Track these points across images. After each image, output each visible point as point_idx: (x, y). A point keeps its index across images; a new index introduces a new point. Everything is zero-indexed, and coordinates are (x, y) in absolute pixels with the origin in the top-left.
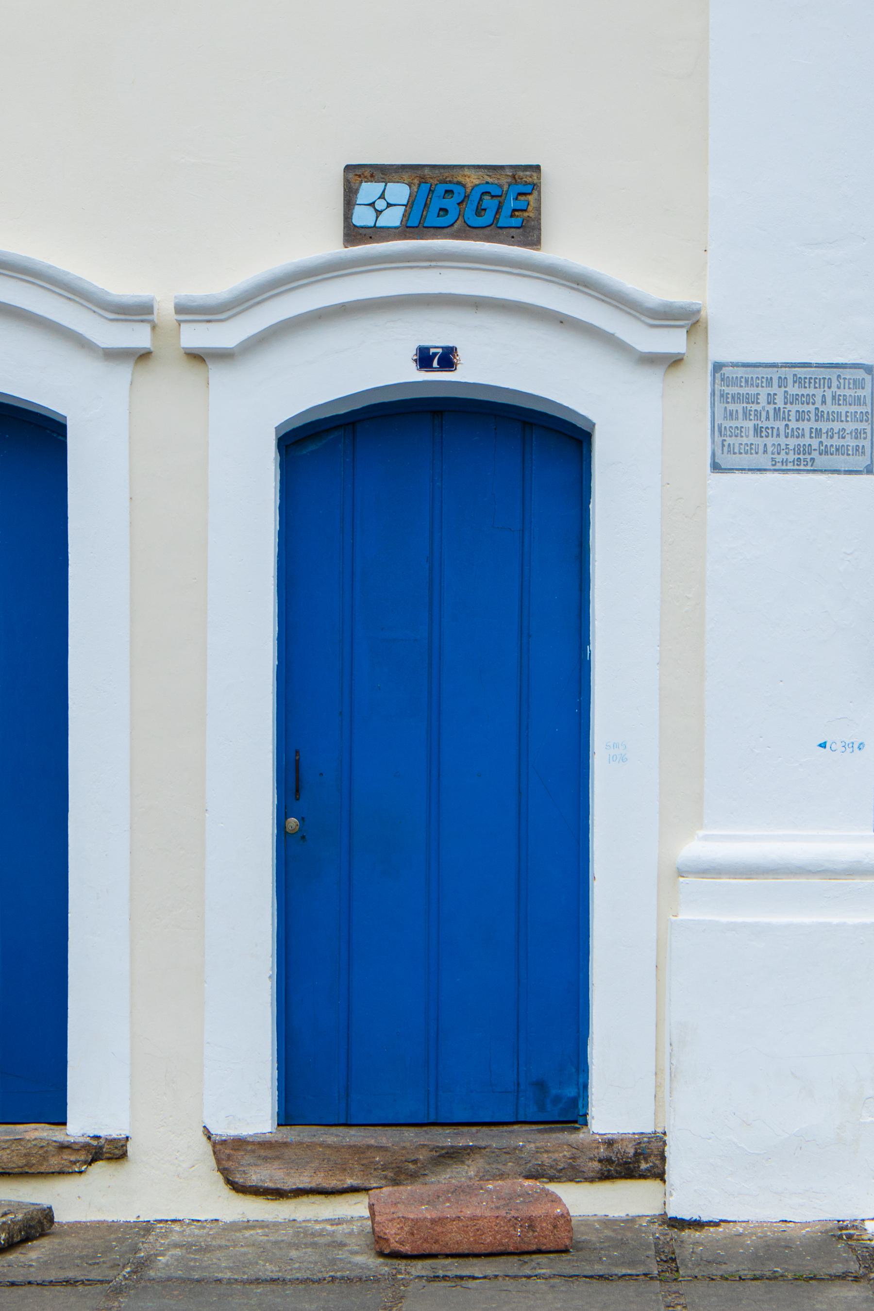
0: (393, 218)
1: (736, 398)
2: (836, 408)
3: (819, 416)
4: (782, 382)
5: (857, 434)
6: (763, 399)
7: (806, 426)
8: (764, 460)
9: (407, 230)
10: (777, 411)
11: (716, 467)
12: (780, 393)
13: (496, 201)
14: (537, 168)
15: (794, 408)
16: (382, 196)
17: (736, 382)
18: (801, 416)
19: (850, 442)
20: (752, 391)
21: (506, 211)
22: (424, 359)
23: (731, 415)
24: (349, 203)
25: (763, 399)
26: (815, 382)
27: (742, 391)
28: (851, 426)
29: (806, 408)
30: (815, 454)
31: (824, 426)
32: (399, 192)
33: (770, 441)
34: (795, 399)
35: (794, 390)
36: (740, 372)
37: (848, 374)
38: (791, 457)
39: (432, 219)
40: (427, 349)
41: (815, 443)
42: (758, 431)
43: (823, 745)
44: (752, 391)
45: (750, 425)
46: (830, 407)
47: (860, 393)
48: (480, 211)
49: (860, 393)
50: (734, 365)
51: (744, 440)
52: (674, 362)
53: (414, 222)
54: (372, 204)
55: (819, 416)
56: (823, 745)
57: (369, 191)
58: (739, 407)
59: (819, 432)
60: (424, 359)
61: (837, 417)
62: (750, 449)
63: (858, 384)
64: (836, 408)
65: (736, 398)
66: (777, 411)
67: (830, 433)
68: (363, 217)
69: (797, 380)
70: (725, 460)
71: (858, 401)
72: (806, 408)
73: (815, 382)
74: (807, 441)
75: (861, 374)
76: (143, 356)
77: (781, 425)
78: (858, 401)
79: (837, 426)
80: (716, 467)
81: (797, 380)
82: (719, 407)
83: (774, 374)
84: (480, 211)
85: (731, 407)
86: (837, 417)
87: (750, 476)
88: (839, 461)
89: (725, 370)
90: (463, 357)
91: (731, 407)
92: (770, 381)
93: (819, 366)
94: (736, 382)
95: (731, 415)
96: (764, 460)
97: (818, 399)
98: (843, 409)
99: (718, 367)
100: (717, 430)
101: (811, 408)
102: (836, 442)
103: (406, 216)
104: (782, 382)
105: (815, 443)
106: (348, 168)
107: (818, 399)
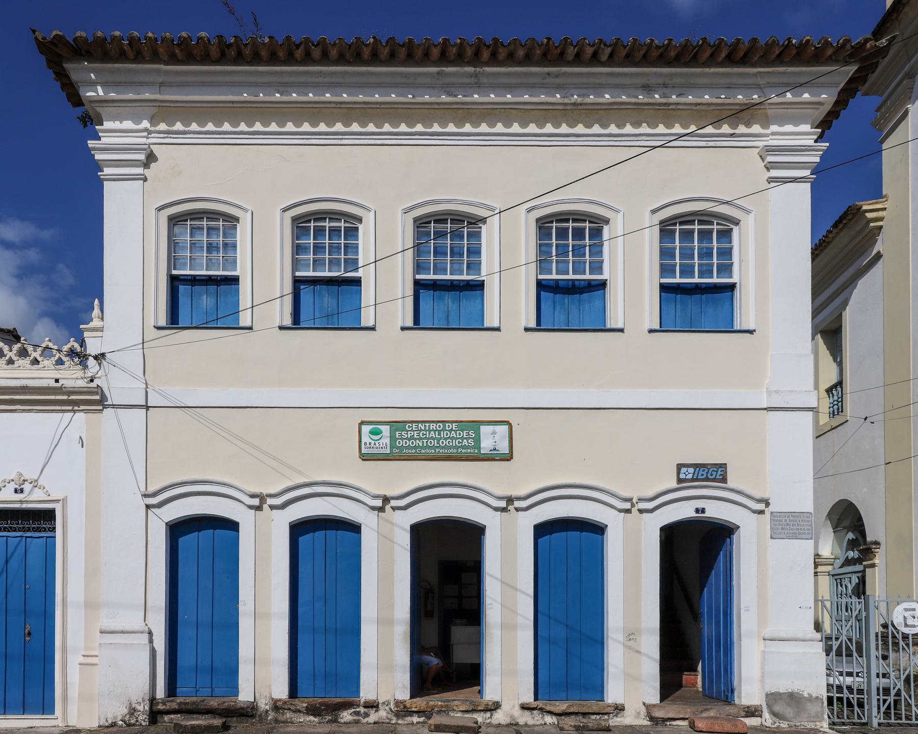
1: (777, 521)
2: (802, 523)
3: (798, 525)
4: (789, 517)
5: (808, 530)
6: (784, 521)
7: (795, 527)
8: (784, 536)
9: (693, 480)
10: (787, 524)
11: (772, 538)
12: (788, 519)
13: (716, 472)
14: (726, 464)
16: (687, 471)
17: (777, 517)
18: (793, 525)
21: (718, 475)
22: (697, 511)
23: (775, 525)
24: (678, 473)
25: (784, 521)
26: (797, 517)
27: (778, 519)
29: (794, 523)
30: (797, 535)
31: (799, 527)
32: (691, 470)
33: (785, 531)
34: (792, 521)
36: (778, 514)
37: (805, 514)
38: (791, 535)
39: (700, 477)
40: (698, 508)
41: (797, 532)
42: (782, 529)
43: (800, 608)
44: (781, 519)
45: (781, 527)
46: (801, 523)
47: (809, 519)
48: (712, 475)
49: (809, 519)
50: (776, 512)
51: (779, 531)
52: (761, 512)
53: (695, 477)
54: (685, 473)
55: (798, 525)
56: (800, 608)
57: (684, 470)
59: (798, 529)
60: (697, 511)
61: (803, 525)
63: (808, 517)
64: (802, 523)
65: (777, 521)
66: (787, 524)
67: (801, 529)
68: (682, 476)
69: (792, 516)
70: (774, 536)
71: (808, 521)
72: (794, 523)
73: (797, 517)
74: (795, 531)
75: (809, 515)
76: (628, 511)
77: (788, 527)
78: (808, 521)
79: (803, 527)
80: (772, 538)
81: (792, 516)
82: (773, 522)
84: (712, 475)
85: (776, 523)
86: (803, 525)
87: (781, 540)
89: (774, 514)
91: (776, 523)
92: (785, 516)
93: (798, 513)
94: (777, 517)
95: (775, 525)
96: (784, 536)
97: (798, 521)
98: (804, 523)
99: (772, 513)
101: (796, 523)
102: (803, 531)
103: (693, 476)
104: (789, 517)
105: (797, 532)
106: (678, 465)
107: (798, 521)
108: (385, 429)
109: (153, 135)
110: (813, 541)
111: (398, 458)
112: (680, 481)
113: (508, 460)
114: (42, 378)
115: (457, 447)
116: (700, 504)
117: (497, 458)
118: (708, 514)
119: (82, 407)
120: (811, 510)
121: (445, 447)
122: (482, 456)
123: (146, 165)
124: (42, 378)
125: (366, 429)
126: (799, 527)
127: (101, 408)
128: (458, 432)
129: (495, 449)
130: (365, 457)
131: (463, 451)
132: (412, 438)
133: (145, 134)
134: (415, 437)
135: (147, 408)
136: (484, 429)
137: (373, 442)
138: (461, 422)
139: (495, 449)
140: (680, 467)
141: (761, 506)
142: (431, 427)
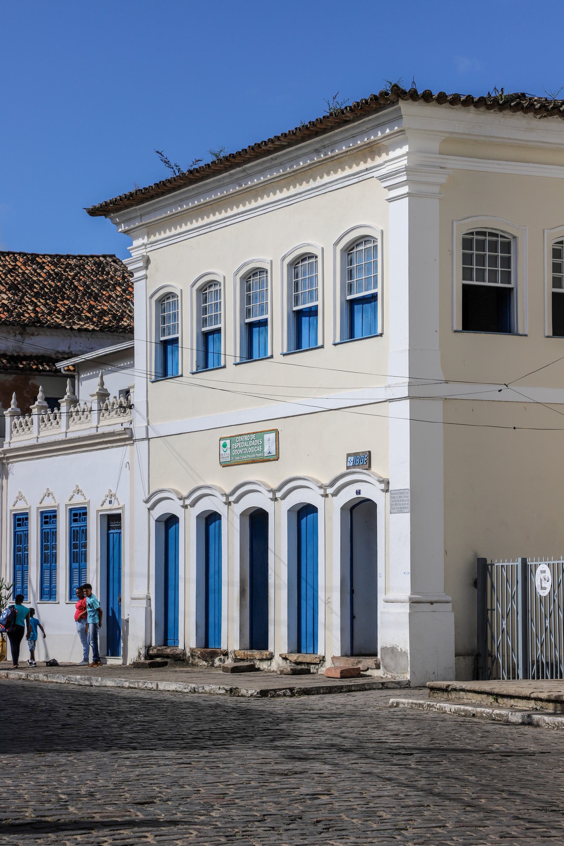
0: (351, 464)
9: (354, 466)
15: (400, 499)
19: (407, 506)
20: (394, 496)
26: (403, 493)
28: (407, 502)
31: (404, 503)
35: (400, 495)
44: (394, 496)
46: (404, 499)
58: (393, 499)
62: (395, 508)
69: (400, 493)
71: (407, 497)
73: (403, 493)
77: (398, 503)
79: (405, 502)
83: (397, 492)
88: (404, 510)
90: (362, 492)
99: (391, 491)
100: (391, 505)
102: (405, 506)
108: (228, 442)
109: (148, 246)
110: (409, 514)
111: (233, 463)
112: (348, 468)
113: (277, 460)
114: (117, 424)
115: (254, 453)
116: (357, 486)
117: (271, 459)
118: (363, 495)
119: (127, 443)
120: (408, 487)
121: (250, 454)
122: (266, 458)
123: (147, 268)
124: (117, 424)
125: (222, 442)
126: (404, 503)
127: (132, 442)
128: (256, 441)
129: (270, 453)
130: (225, 465)
131: (258, 455)
132: (238, 448)
133: (144, 247)
134: (240, 447)
135: (149, 439)
136: (266, 436)
137: (224, 453)
138: (257, 432)
139: (270, 453)
140: (349, 455)
141: (382, 486)
142: (246, 438)
